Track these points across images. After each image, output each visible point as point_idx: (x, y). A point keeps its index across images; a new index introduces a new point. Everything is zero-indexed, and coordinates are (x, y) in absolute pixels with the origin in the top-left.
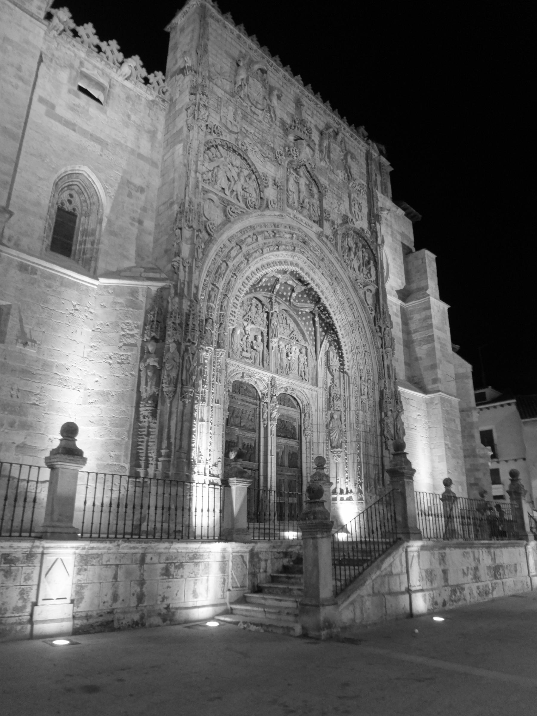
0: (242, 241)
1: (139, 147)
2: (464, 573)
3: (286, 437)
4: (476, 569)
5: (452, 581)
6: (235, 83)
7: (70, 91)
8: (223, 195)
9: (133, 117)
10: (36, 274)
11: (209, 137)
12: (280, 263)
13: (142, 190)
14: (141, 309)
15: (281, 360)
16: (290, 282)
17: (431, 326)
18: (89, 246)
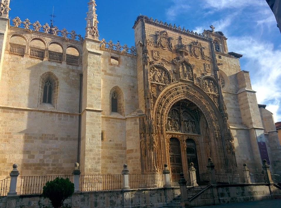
0: (165, 96)
1: (131, 74)
2: (237, 194)
3: (191, 153)
4: (243, 192)
5: (232, 195)
6: (156, 42)
7: (109, 65)
8: (157, 83)
9: (128, 65)
10: (110, 121)
11: (151, 66)
12: (180, 98)
13: (133, 87)
14: (138, 124)
15: (186, 128)
16: (185, 102)
17: (248, 102)
18: (122, 108)
